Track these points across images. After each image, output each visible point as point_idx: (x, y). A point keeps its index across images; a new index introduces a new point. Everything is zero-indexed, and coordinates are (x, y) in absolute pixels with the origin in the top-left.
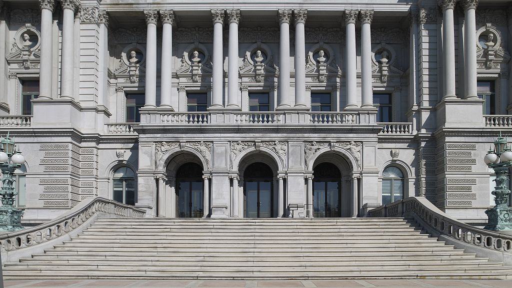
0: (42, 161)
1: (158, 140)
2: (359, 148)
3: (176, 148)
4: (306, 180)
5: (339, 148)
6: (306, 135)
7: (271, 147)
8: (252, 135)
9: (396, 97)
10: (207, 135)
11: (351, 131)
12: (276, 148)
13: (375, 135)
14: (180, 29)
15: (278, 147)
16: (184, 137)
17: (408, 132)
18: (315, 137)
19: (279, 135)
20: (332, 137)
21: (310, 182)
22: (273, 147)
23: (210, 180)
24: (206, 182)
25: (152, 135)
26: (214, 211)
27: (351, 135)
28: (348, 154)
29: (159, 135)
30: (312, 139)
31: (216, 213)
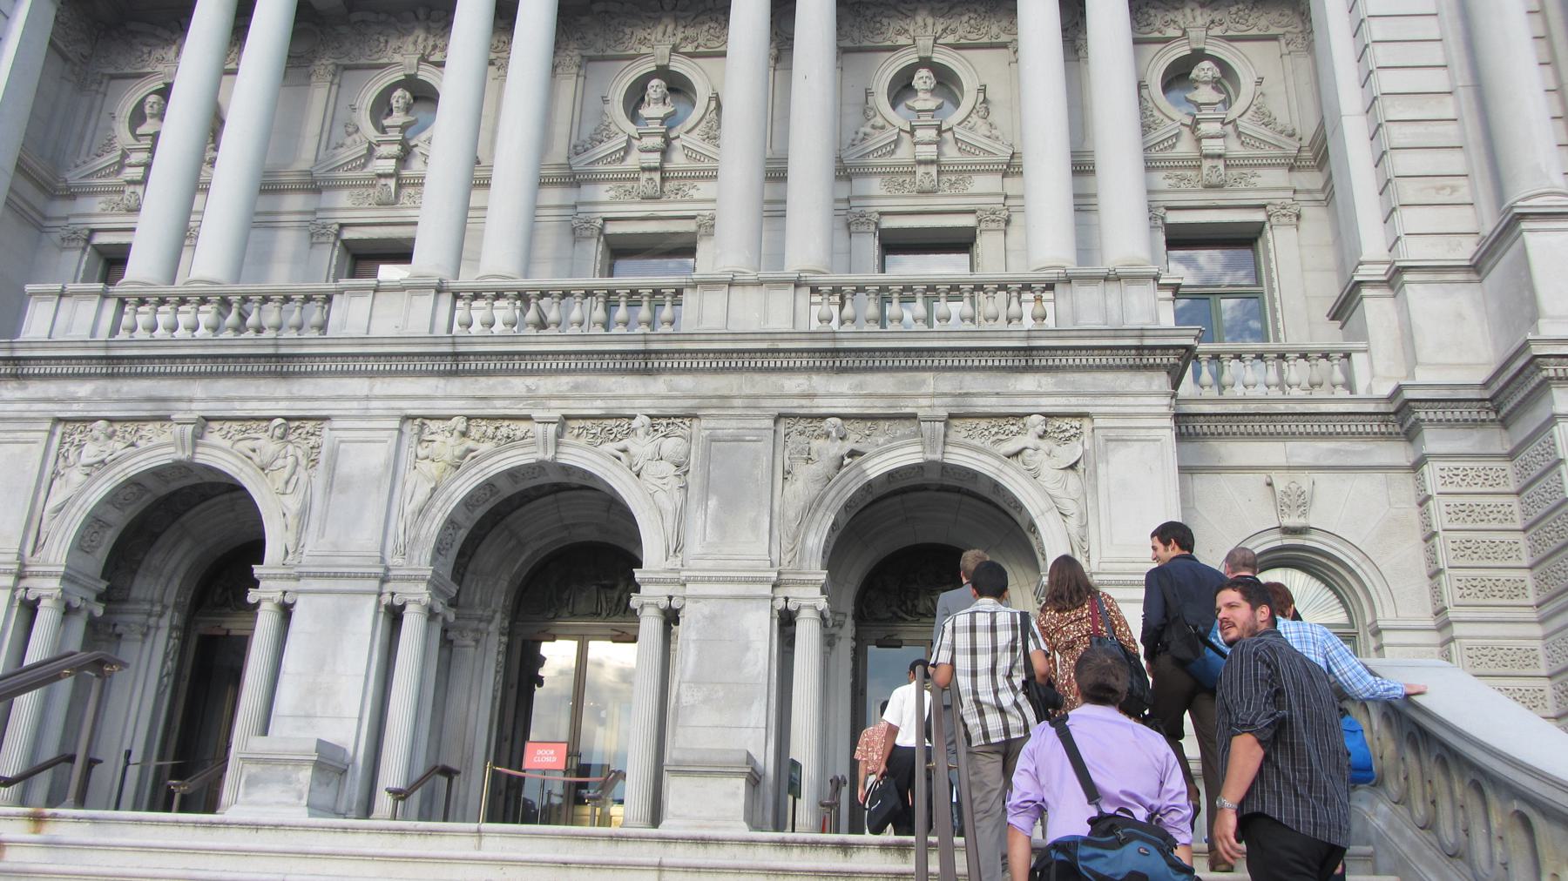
1: (76, 410)
3: (158, 449)
4: (787, 621)
5: (971, 454)
6: (794, 384)
7: (611, 447)
8: (518, 385)
12: (633, 449)
14: (356, 16)
18: (839, 393)
19: (659, 385)
20: (929, 392)
21: (807, 634)
22: (621, 445)
23: (286, 611)
24: (266, 622)
25: (52, 389)
26: (252, 782)
27: (1028, 382)
28: (1015, 482)
29: (84, 389)
30: (822, 406)
31: (258, 795)
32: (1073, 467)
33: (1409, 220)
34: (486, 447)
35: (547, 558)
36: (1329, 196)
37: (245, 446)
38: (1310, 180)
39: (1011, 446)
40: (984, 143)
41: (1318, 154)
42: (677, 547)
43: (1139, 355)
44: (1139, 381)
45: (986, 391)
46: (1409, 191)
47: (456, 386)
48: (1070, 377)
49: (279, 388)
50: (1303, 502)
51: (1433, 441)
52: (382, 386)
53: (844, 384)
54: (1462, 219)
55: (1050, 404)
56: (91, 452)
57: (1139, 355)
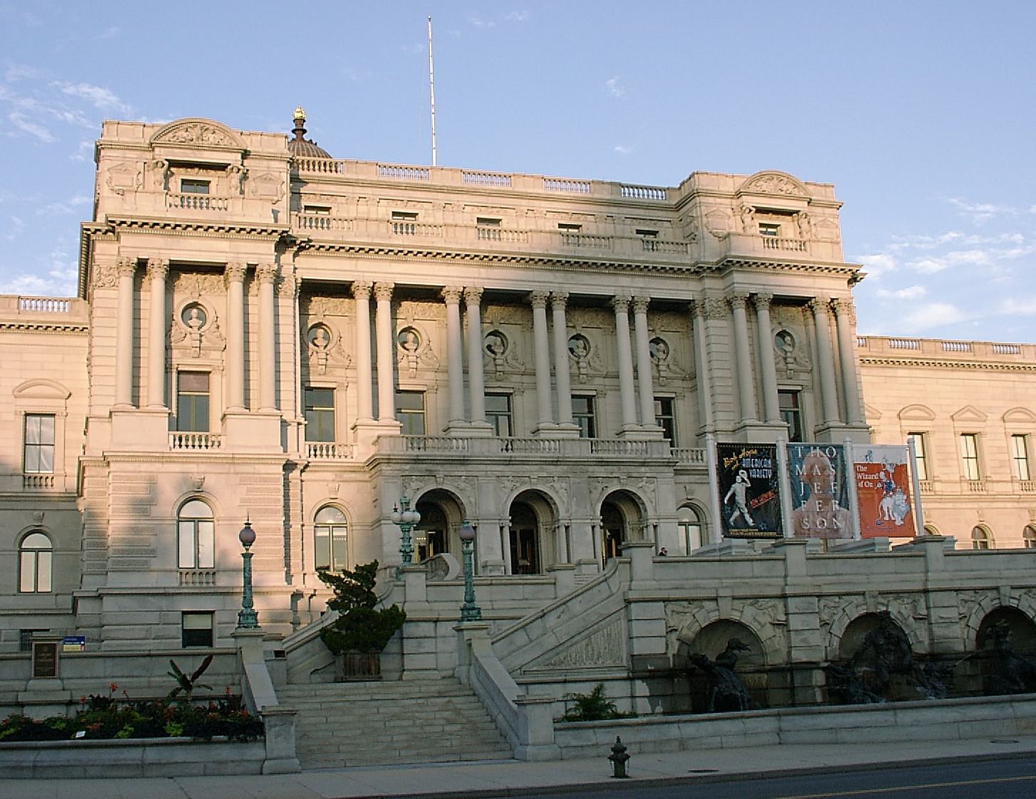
0: (242, 500)
1: (407, 473)
2: (652, 487)
6: (591, 469)
7: (549, 485)
9: (682, 410)
10: (470, 468)
11: (643, 464)
13: (671, 469)
15: (557, 485)
16: (441, 470)
17: (702, 460)
18: (601, 471)
19: (559, 468)
27: (643, 469)
29: (408, 467)
32: (653, 491)
33: (720, 416)
34: (518, 485)
35: (527, 514)
36: (694, 389)
37: (456, 484)
38: (688, 384)
39: (640, 485)
40: (599, 367)
41: (693, 377)
42: (567, 511)
43: (668, 464)
44: (666, 469)
45: (635, 471)
46: (719, 407)
47: (508, 468)
48: (653, 468)
49: (463, 468)
50: (692, 492)
52: (489, 467)
53: (602, 469)
54: (731, 416)
55: (648, 475)
56: (414, 485)
57: (668, 464)
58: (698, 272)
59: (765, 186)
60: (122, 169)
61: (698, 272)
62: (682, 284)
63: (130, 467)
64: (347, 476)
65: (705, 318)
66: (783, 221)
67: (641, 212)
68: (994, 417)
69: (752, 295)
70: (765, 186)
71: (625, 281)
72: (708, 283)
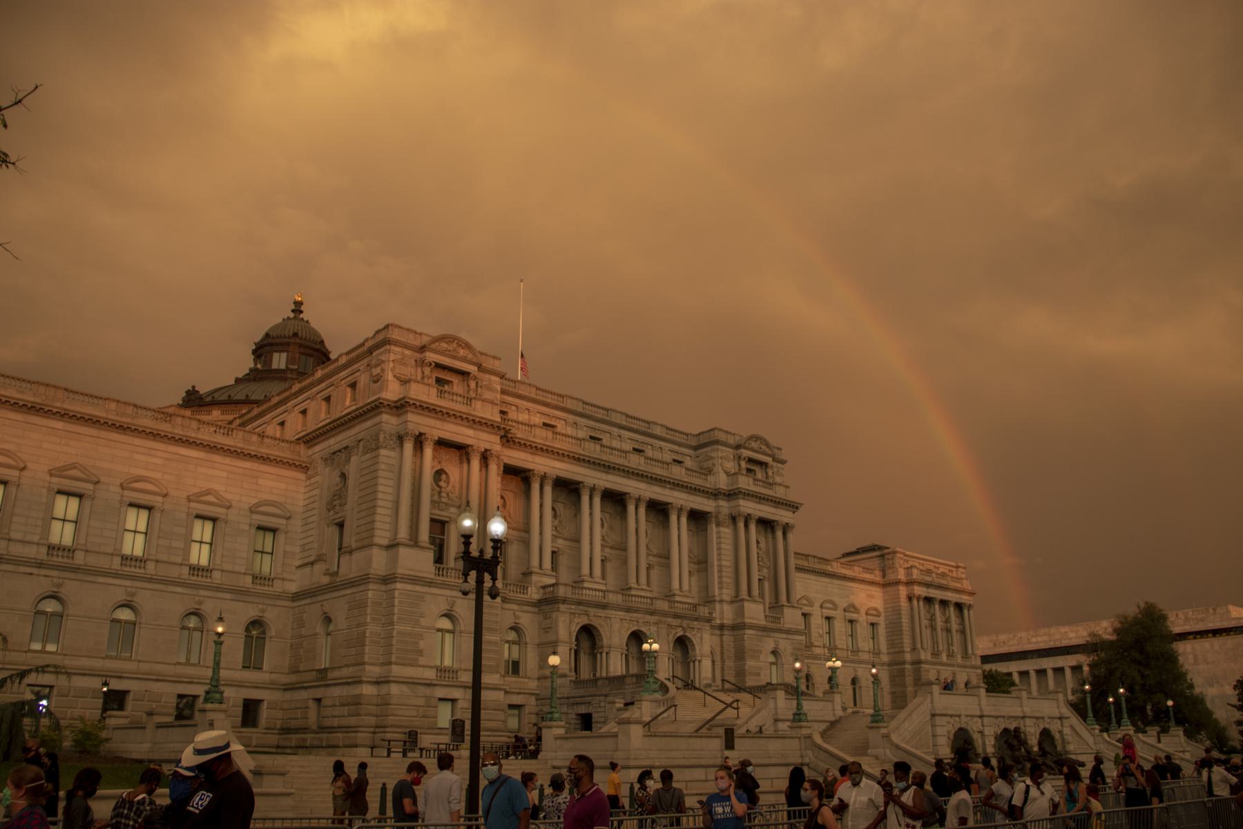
3: (584, 621)
16: (592, 611)
33: (725, 591)
51: (726, 632)
58: (715, 494)
59: (754, 445)
60: (402, 361)
61: (715, 494)
62: (705, 501)
63: (409, 587)
64: (526, 608)
65: (718, 525)
66: (455, 379)
67: (676, 448)
68: (817, 605)
69: (421, 434)
70: (754, 445)
71: (677, 494)
72: (722, 503)
